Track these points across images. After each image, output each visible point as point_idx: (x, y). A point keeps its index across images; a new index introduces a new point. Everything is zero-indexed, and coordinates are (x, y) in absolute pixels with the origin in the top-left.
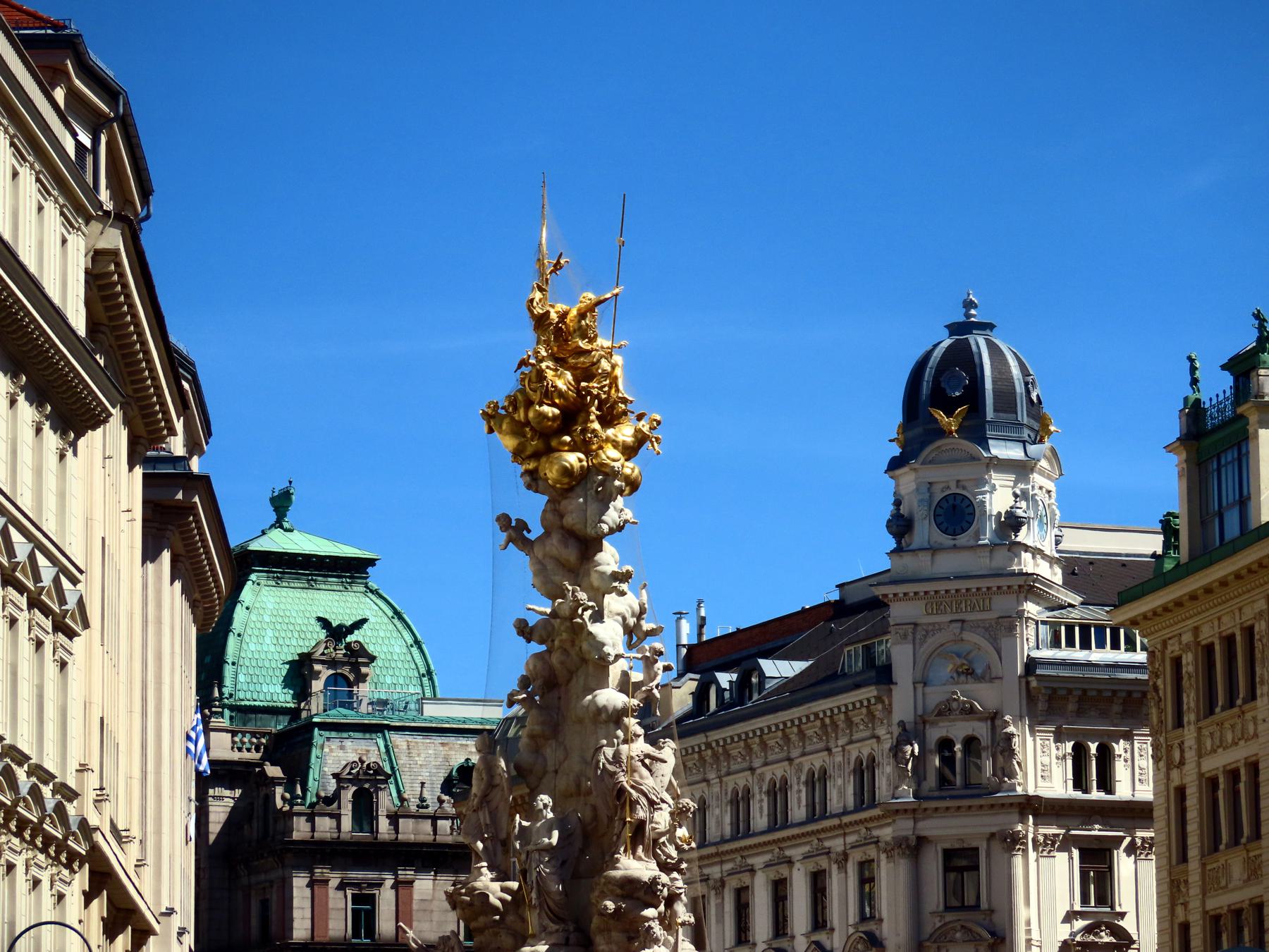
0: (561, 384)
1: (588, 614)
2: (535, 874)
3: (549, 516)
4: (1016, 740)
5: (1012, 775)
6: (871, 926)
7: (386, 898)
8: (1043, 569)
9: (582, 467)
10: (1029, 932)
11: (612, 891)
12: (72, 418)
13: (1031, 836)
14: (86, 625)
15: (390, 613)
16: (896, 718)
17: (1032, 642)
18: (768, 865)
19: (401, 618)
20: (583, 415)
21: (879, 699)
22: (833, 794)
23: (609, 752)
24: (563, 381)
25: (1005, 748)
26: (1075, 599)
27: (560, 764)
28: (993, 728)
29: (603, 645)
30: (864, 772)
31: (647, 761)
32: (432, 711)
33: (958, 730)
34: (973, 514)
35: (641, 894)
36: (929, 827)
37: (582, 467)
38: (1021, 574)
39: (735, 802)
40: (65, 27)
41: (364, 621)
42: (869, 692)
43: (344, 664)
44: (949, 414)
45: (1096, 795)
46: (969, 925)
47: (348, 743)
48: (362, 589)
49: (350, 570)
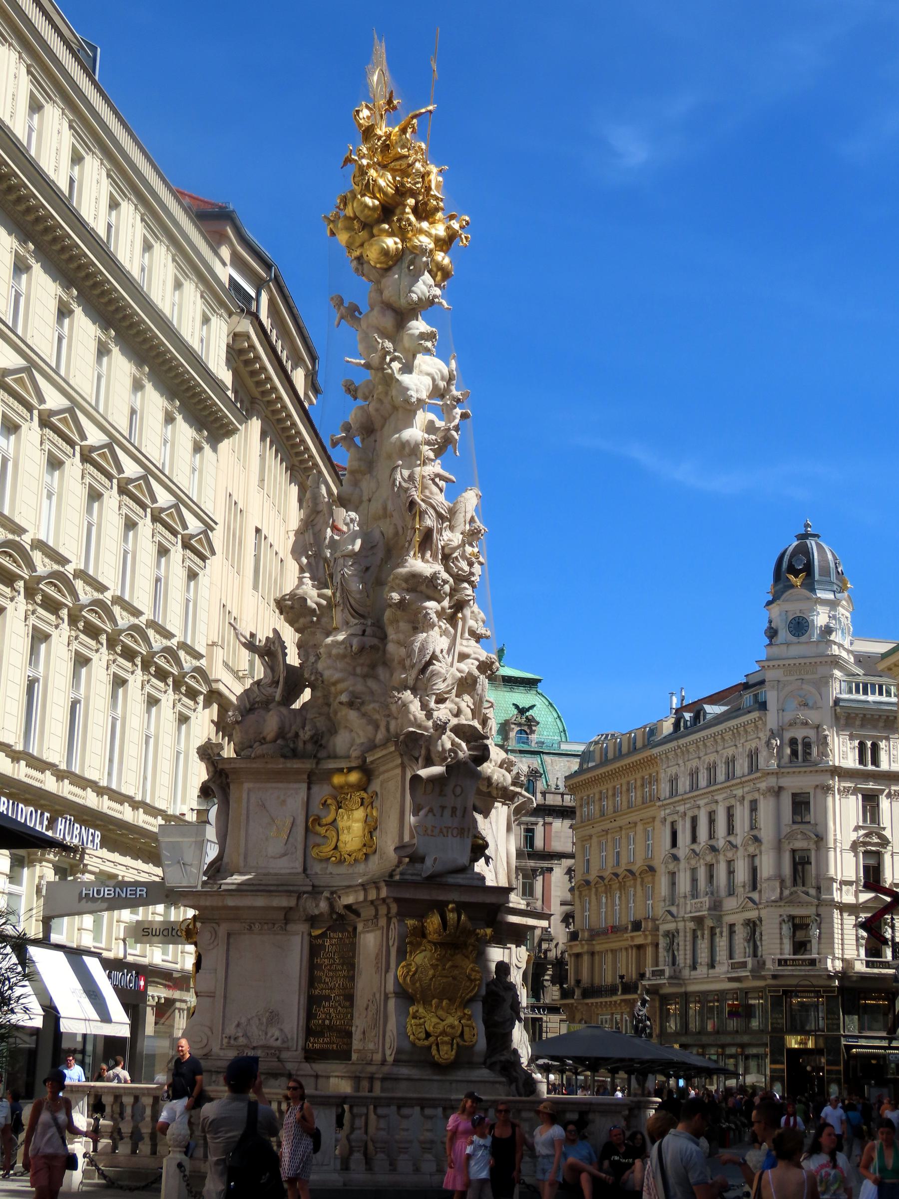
0: (382, 182)
1: (396, 365)
2: (339, 576)
3: (373, 294)
4: (829, 738)
5: (827, 756)
6: (755, 832)
7: (539, 831)
8: (844, 654)
9: (397, 249)
10: (835, 835)
11: (399, 585)
12: (212, 427)
13: (836, 787)
14: (213, 553)
16: (769, 727)
17: (838, 689)
18: (706, 804)
19: (552, 706)
20: (400, 207)
21: (760, 718)
22: (737, 767)
23: (406, 473)
24: (385, 181)
25: (823, 742)
26: (860, 671)
27: (373, 493)
28: (818, 732)
29: (408, 389)
30: (753, 756)
31: (437, 480)
32: (565, 747)
33: (799, 734)
34: (808, 626)
35: (423, 588)
36: (785, 782)
37: (397, 249)
38: (832, 655)
39: (691, 775)
40: (226, 208)
41: (534, 706)
42: (755, 715)
43: (525, 725)
44: (796, 577)
45: (870, 767)
46: (808, 833)
47: (524, 759)
49: (529, 684)
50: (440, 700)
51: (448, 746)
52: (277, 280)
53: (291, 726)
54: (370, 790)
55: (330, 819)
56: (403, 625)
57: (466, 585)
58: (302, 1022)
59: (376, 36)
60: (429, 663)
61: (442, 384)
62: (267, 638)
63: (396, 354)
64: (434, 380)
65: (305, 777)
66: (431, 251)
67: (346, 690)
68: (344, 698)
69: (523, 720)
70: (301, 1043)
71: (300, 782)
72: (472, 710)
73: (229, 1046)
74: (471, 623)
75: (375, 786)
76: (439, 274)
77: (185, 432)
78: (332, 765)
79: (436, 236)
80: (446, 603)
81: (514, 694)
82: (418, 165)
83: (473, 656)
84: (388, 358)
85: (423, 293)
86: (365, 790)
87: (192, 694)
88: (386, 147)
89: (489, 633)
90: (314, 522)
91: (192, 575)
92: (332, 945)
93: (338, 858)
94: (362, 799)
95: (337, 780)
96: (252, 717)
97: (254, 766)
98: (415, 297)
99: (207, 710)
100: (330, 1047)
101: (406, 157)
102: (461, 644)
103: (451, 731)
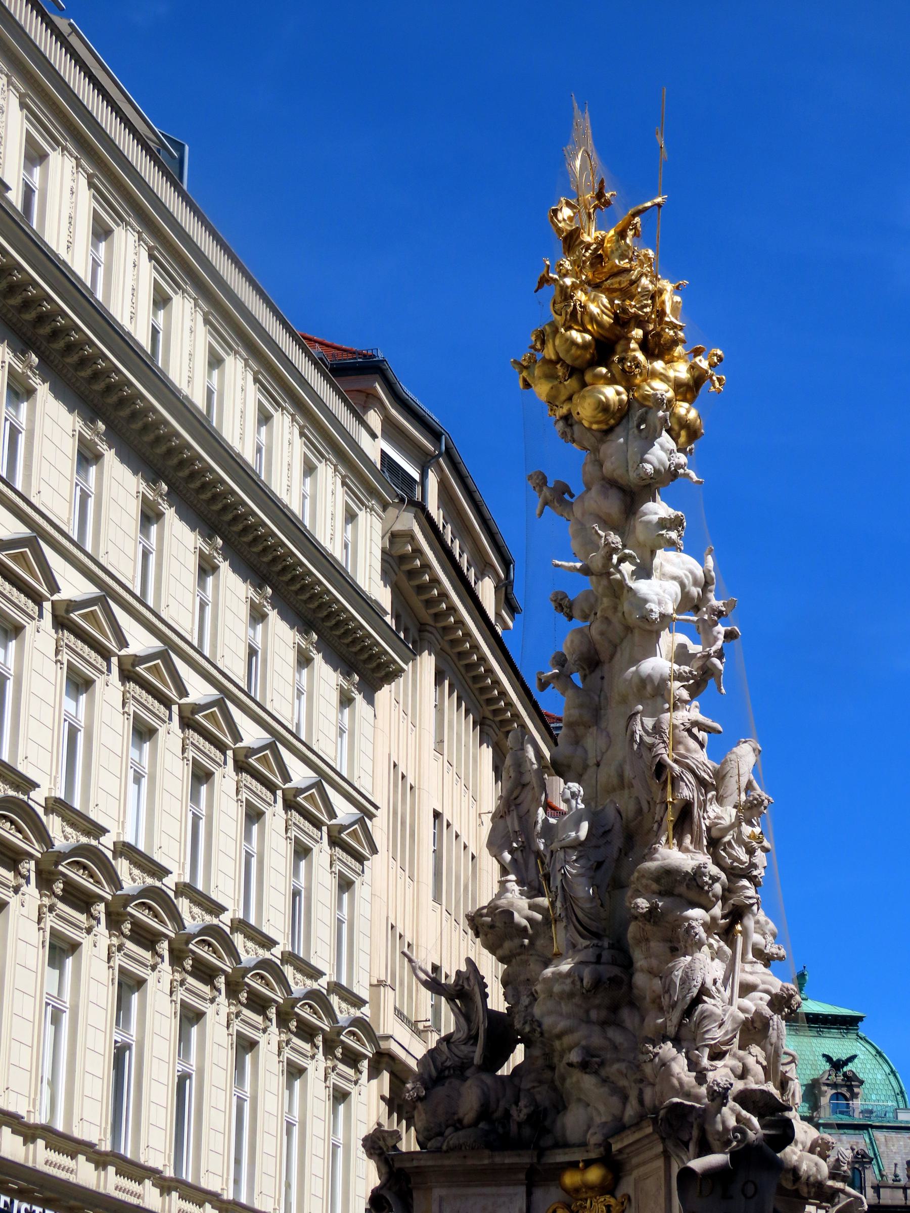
0: (594, 308)
1: (627, 568)
2: (559, 877)
3: (589, 468)
9: (621, 401)
11: (646, 887)
12: (366, 670)
14: (374, 850)
15: (874, 1053)
19: (881, 1055)
20: (622, 342)
23: (649, 722)
24: (598, 306)
27: (603, 754)
29: (646, 601)
31: (695, 730)
35: (682, 889)
37: (621, 401)
40: (374, 356)
43: (842, 1086)
47: (844, 1137)
48: (855, 1036)
49: (846, 1024)
50: (717, 1055)
51: (732, 1122)
52: (449, 455)
53: (498, 1101)
54: (619, 1193)
56: (656, 946)
57: (745, 882)
59: (576, 105)
60: (698, 1000)
61: (695, 591)
62: (458, 973)
63: (627, 551)
64: (683, 586)
65: (522, 1176)
66: (670, 401)
67: (577, 1045)
68: (574, 1057)
69: (840, 1079)
71: (515, 1184)
72: (764, 1068)
74: (756, 938)
75: (627, 1187)
76: (683, 433)
77: (327, 678)
78: (561, 1157)
79: (676, 378)
80: (717, 910)
81: (823, 1040)
82: (645, 281)
83: (761, 987)
84: (615, 558)
85: (661, 463)
86: (612, 1194)
87: (352, 1059)
88: (598, 259)
89: (782, 952)
90: (518, 801)
91: (345, 885)
95: (570, 1179)
96: (441, 1091)
97: (447, 1162)
98: (649, 468)
99: (374, 1082)
101: (627, 271)
102: (743, 971)
103: (735, 1100)
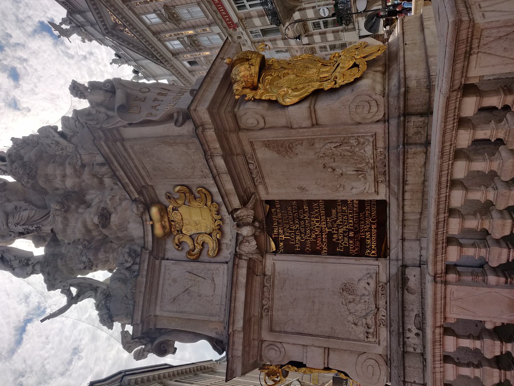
55: (189, 242)
58: (352, 260)
65: (157, 262)
70: (372, 262)
73: (376, 334)
86: (166, 208)
92: (284, 232)
93: (218, 231)
94: (173, 210)
100: (374, 231)
